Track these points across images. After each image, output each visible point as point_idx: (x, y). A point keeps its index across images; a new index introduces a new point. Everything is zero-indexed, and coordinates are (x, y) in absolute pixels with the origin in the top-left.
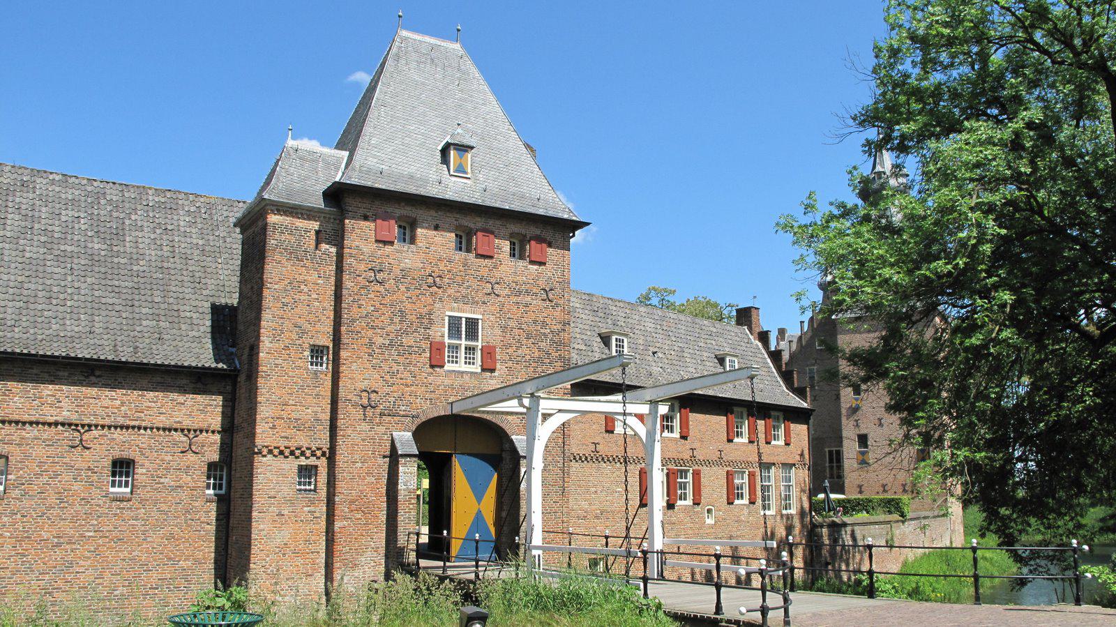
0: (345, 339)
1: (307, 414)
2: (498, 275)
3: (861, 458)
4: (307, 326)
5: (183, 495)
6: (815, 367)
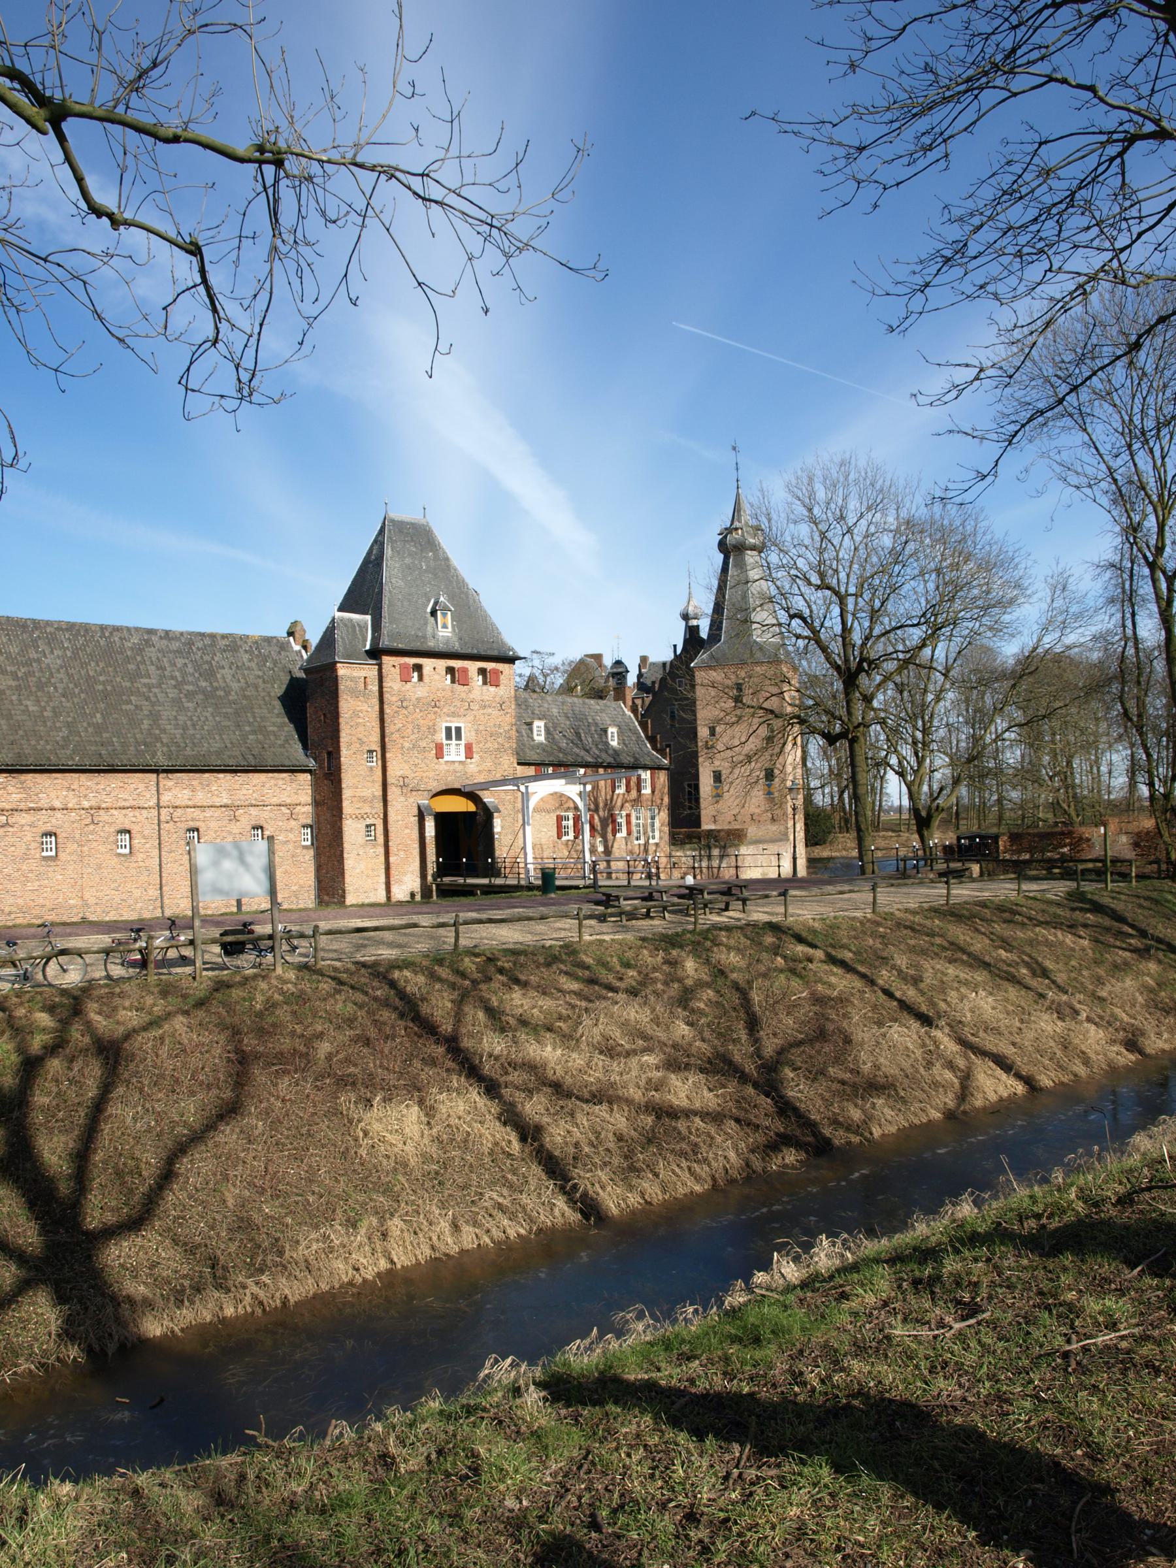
0: (388, 746)
1: (367, 793)
2: (471, 696)
4: (365, 739)
5: (290, 846)
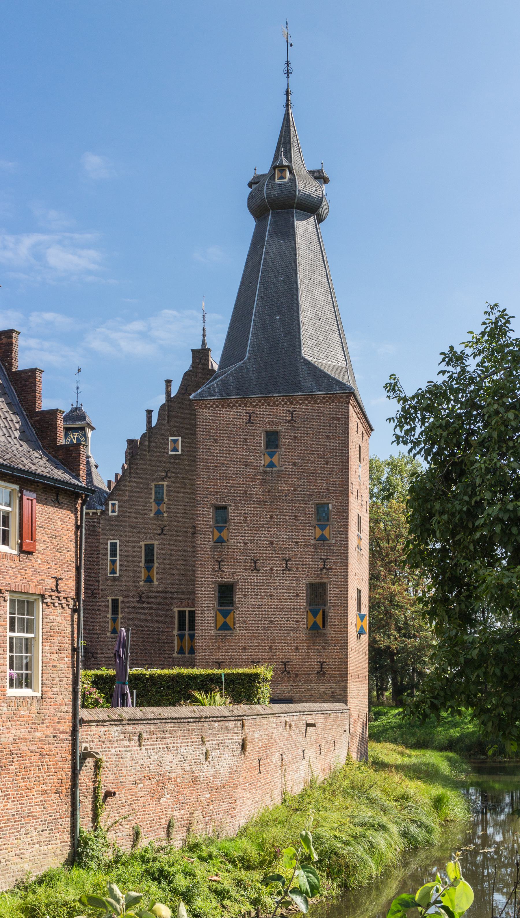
3: (221, 620)
6: (165, 483)
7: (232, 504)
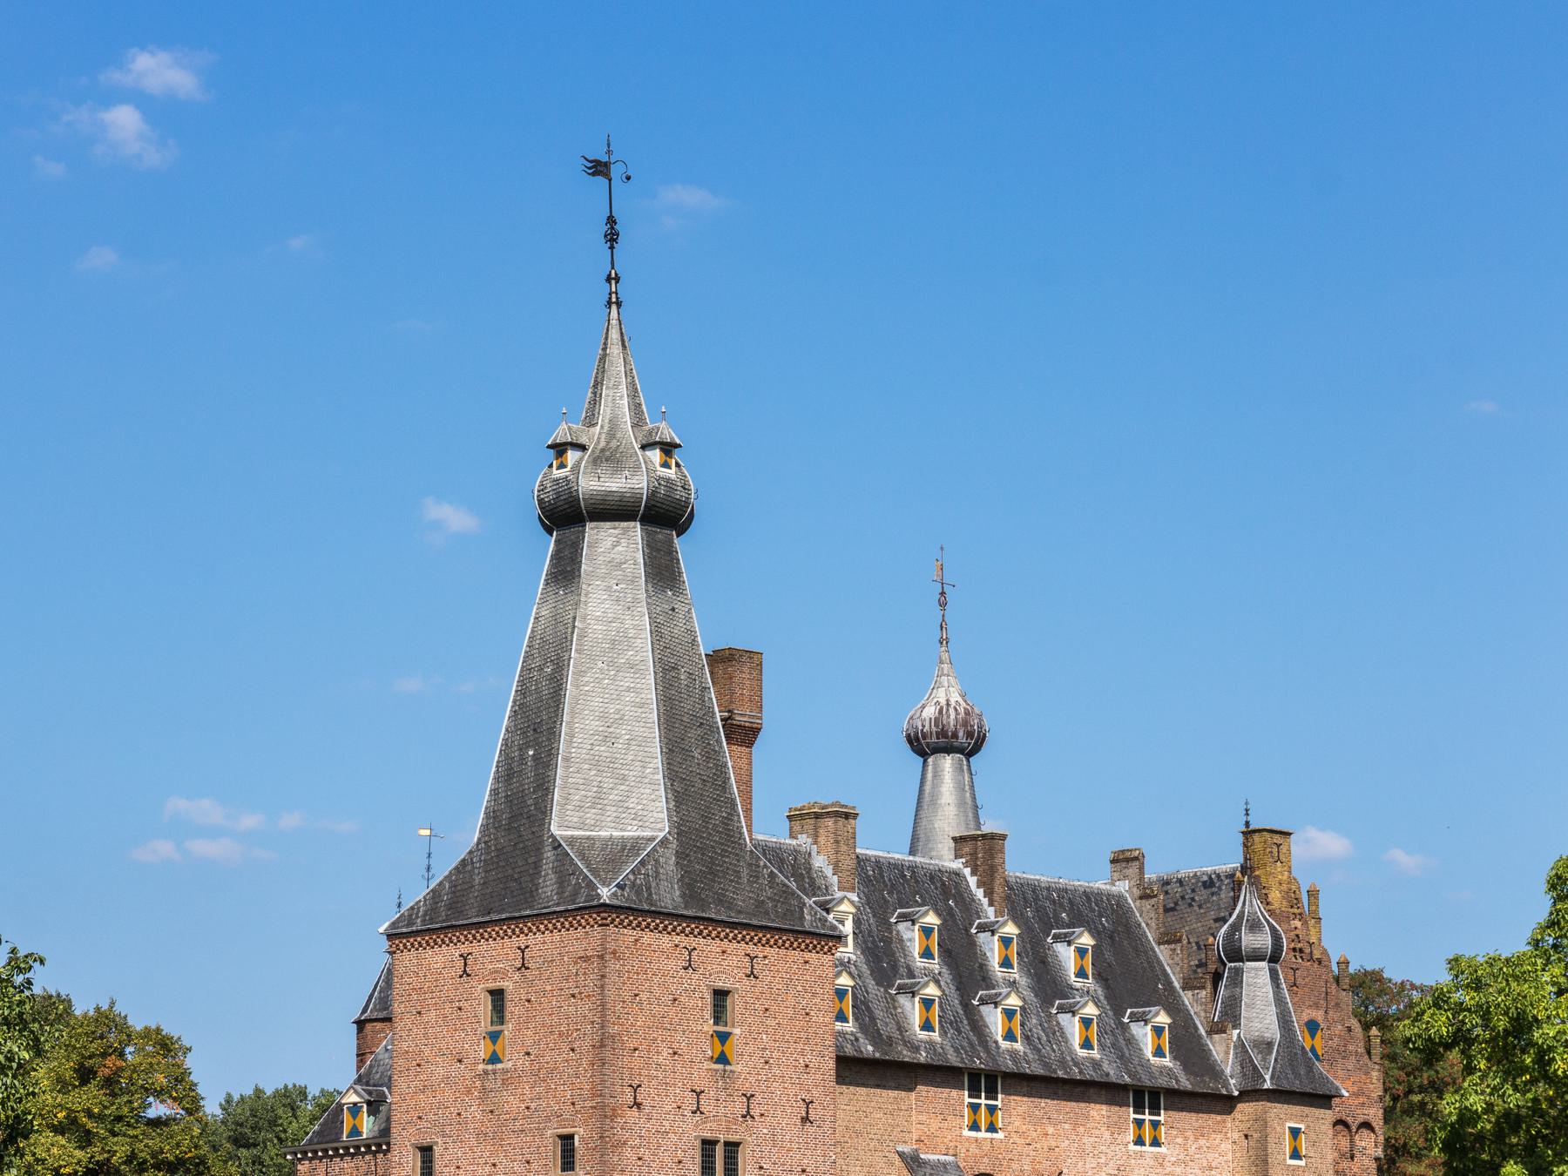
7: (439, 1140)
